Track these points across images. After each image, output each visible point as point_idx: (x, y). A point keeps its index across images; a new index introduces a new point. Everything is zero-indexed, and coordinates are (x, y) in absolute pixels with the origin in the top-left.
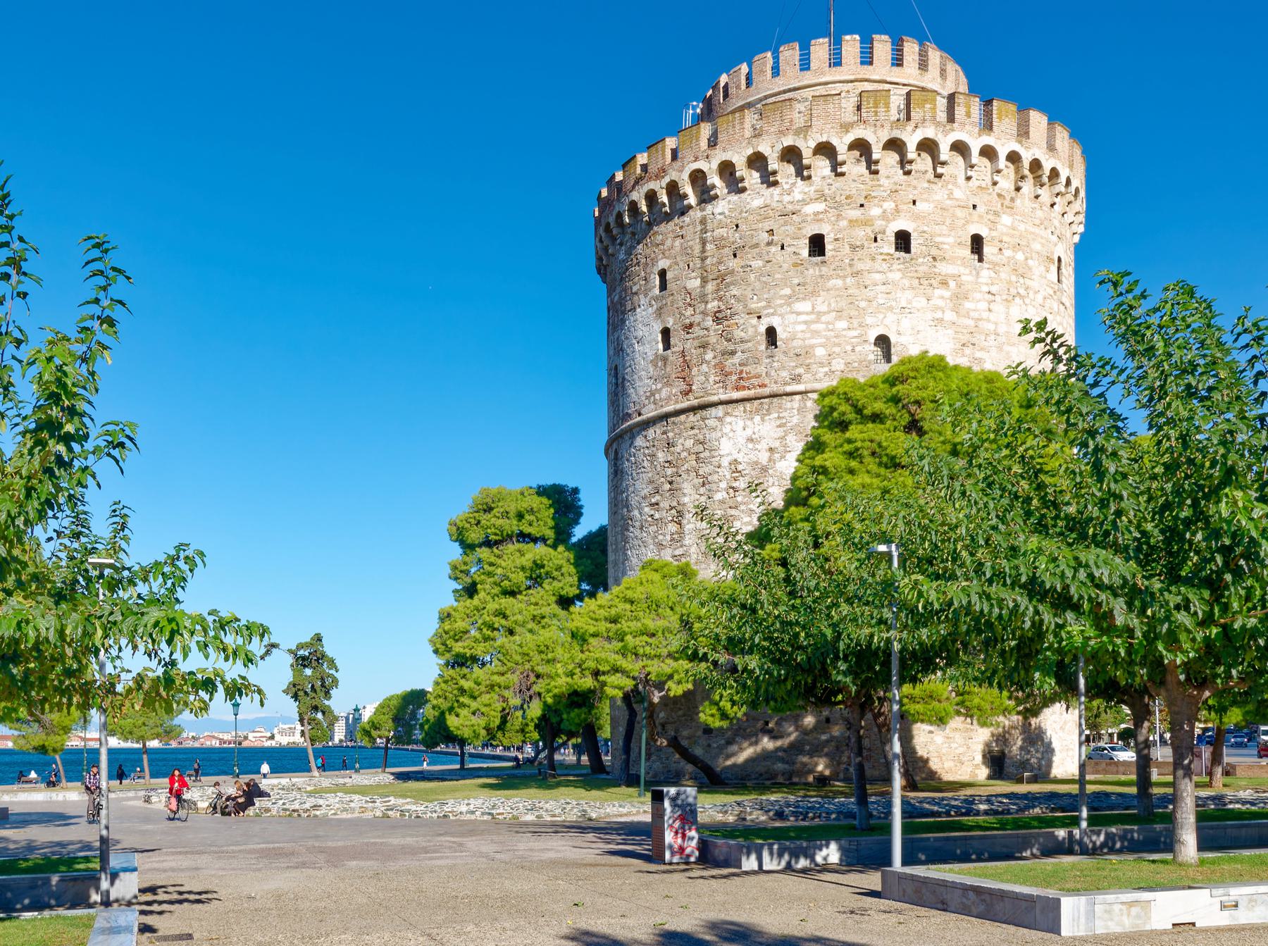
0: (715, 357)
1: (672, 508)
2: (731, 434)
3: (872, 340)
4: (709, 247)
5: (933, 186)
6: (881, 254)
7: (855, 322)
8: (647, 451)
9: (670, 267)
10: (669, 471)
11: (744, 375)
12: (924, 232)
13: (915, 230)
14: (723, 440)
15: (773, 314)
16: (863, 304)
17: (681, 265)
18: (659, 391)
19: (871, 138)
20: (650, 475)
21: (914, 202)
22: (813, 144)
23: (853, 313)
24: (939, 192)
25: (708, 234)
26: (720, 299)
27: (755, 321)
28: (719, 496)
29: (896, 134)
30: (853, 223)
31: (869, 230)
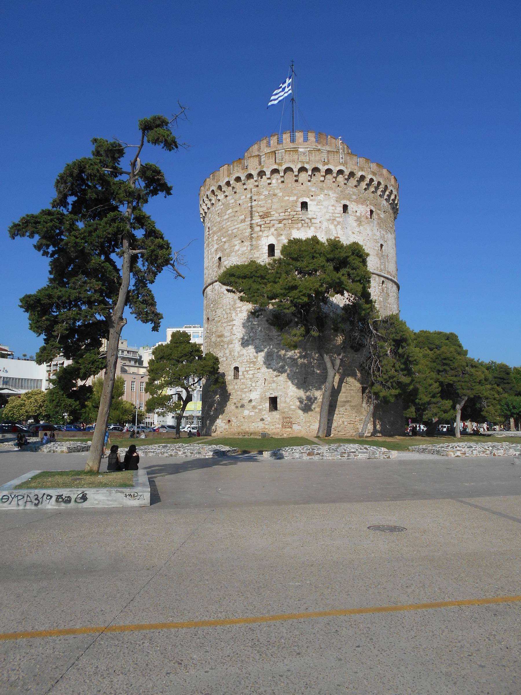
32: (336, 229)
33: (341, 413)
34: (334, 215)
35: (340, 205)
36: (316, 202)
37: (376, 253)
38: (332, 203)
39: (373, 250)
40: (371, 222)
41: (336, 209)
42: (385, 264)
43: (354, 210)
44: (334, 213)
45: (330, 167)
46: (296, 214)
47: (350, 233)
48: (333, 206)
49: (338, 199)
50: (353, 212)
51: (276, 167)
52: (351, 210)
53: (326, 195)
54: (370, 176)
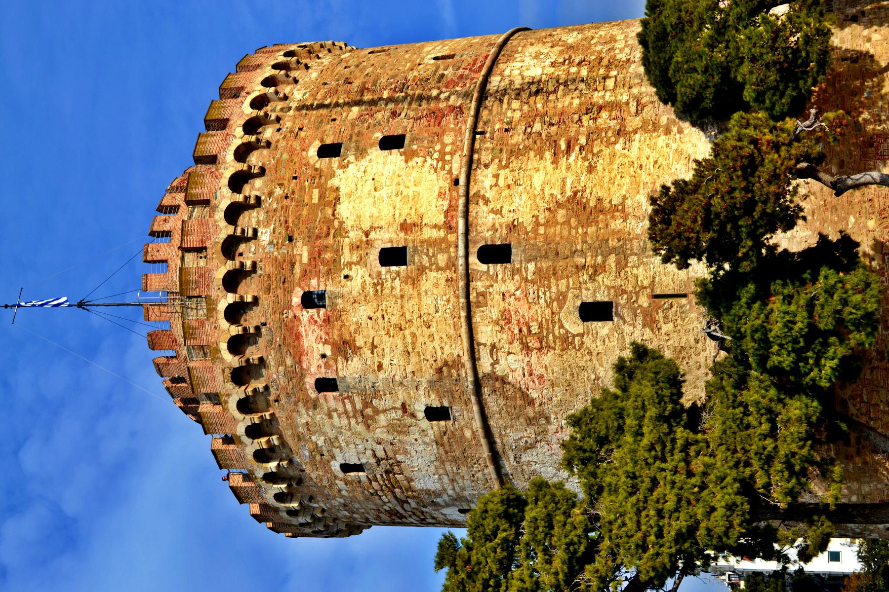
0: (439, 88)
1: (580, 120)
2: (524, 68)
4: (327, 102)
8: (504, 163)
9: (322, 140)
10: (537, 127)
11: (469, 67)
14: (526, 74)
17: (328, 127)
18: (444, 145)
20: (532, 154)
25: (315, 104)
26: (385, 89)
27: (421, 66)
28: (584, 72)
32: (385, 411)
33: (864, 410)
34: (351, 414)
35: (322, 401)
36: (334, 449)
37: (409, 289)
38: (325, 417)
39: (405, 300)
40: (333, 305)
41: (336, 410)
42: (432, 243)
43: (321, 362)
44: (346, 412)
45: (241, 430)
46: (376, 481)
47: (382, 375)
48: (330, 416)
49: (310, 405)
50: (327, 366)
51: (284, 515)
52: (323, 370)
53: (309, 430)
54: (224, 324)
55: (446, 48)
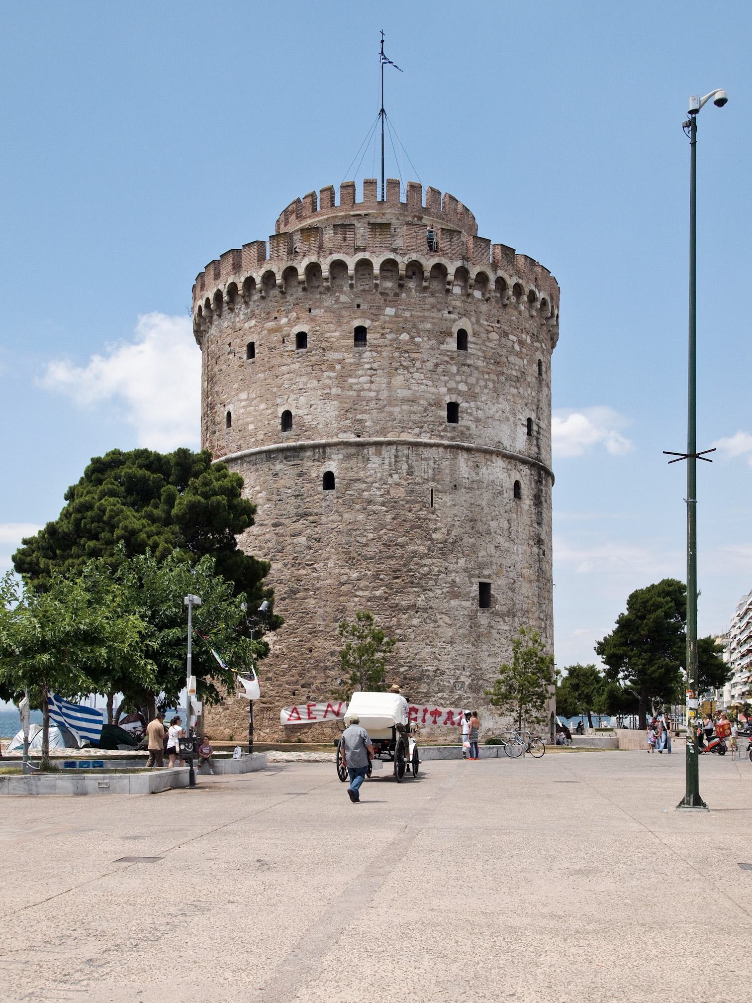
3: (280, 415)
5: (324, 296)
6: (287, 351)
7: (270, 403)
12: (316, 331)
13: (310, 331)
15: (229, 403)
16: (275, 389)
19: (275, 270)
21: (310, 310)
22: (243, 279)
23: (269, 396)
24: (328, 301)
27: (222, 409)
29: (290, 264)
30: (271, 331)
31: (279, 334)
55: (242, 411)
